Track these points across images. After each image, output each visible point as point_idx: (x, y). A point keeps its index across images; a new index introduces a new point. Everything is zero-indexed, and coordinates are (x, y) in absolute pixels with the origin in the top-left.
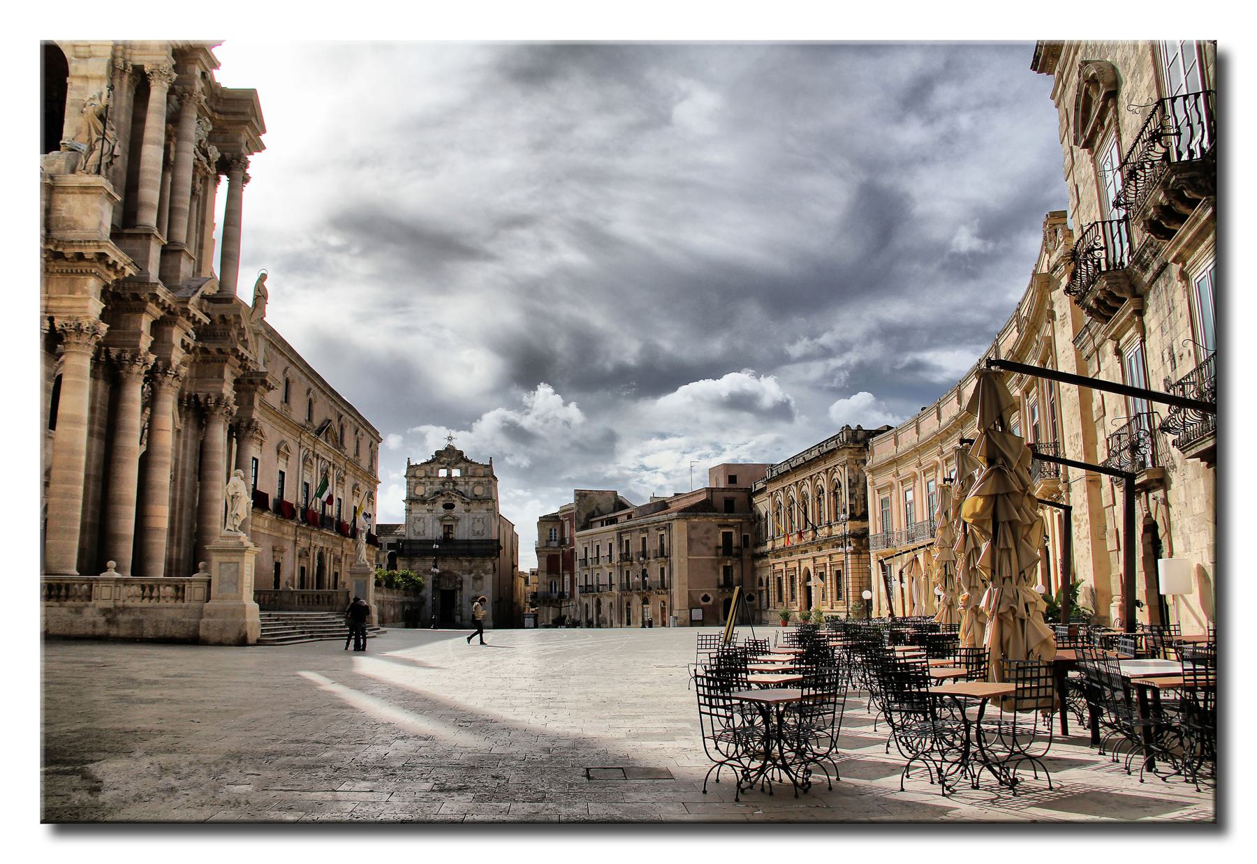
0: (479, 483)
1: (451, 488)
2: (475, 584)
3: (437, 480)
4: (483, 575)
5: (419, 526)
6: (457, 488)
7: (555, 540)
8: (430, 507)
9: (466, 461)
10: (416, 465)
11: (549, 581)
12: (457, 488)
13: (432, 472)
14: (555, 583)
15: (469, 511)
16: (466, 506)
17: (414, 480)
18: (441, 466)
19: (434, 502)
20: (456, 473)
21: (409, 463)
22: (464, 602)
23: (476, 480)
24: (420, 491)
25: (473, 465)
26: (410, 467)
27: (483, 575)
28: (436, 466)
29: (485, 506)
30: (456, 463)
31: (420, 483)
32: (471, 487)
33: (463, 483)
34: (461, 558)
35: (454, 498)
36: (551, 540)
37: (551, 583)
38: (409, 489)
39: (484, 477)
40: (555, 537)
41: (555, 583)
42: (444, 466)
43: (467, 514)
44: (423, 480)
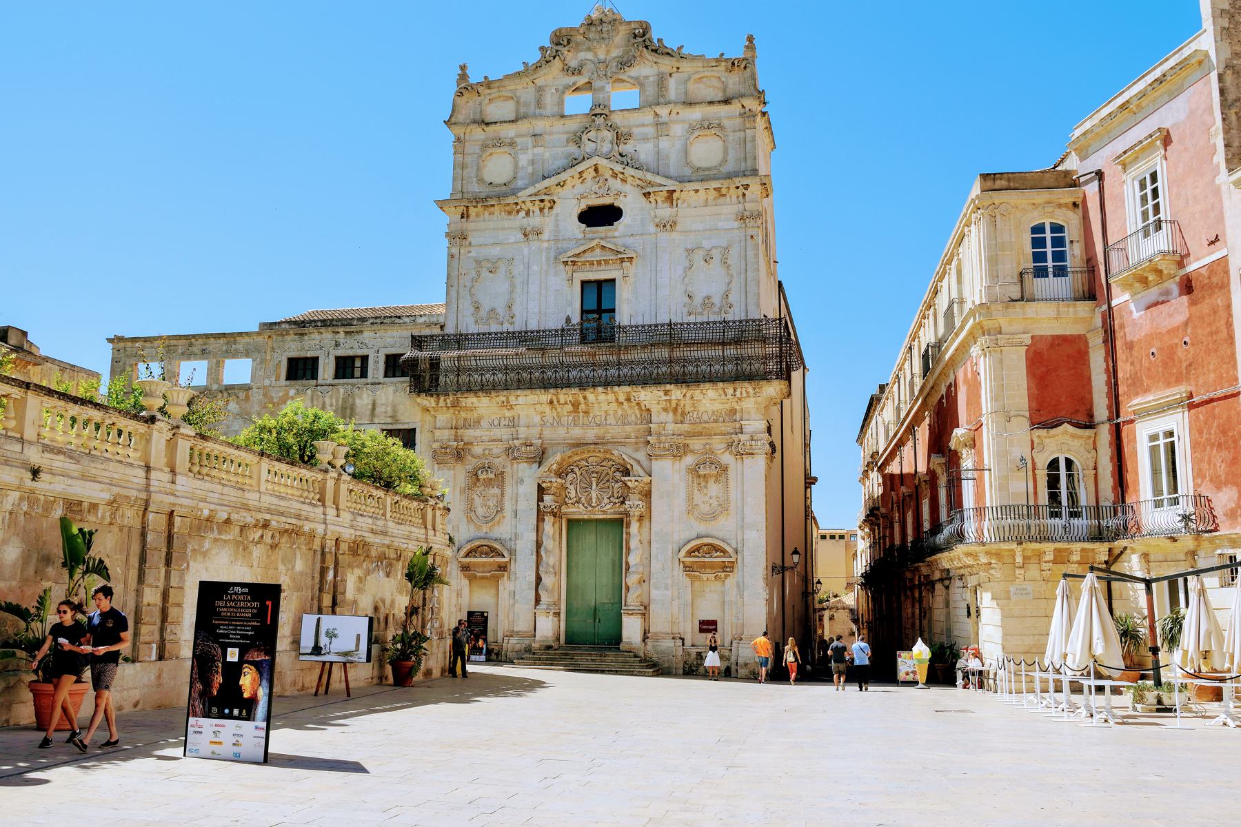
0: (707, 126)
1: (606, 147)
2: (698, 498)
3: (559, 125)
4: (727, 458)
5: (493, 293)
6: (627, 148)
7: (1060, 272)
8: (535, 220)
9: (659, 50)
10: (488, 84)
11: (1043, 461)
12: (627, 148)
13: (539, 103)
14: (1069, 463)
15: (673, 225)
16: (665, 212)
17: (478, 133)
18: (570, 80)
19: (547, 203)
20: (622, 97)
21: (463, 76)
22: (655, 566)
23: (696, 114)
24: (498, 168)
25: (686, 67)
26: (465, 87)
27: (727, 458)
28: (552, 76)
29: (730, 207)
30: (624, 63)
31: (499, 143)
32: (678, 145)
33: (651, 131)
34: (649, 396)
35: (616, 184)
36: (1040, 272)
37: (1054, 464)
38: (460, 166)
39: (726, 102)
40: (1059, 256)
41: (1069, 463)
42: (581, 80)
43: (664, 236)
44: (509, 131)
